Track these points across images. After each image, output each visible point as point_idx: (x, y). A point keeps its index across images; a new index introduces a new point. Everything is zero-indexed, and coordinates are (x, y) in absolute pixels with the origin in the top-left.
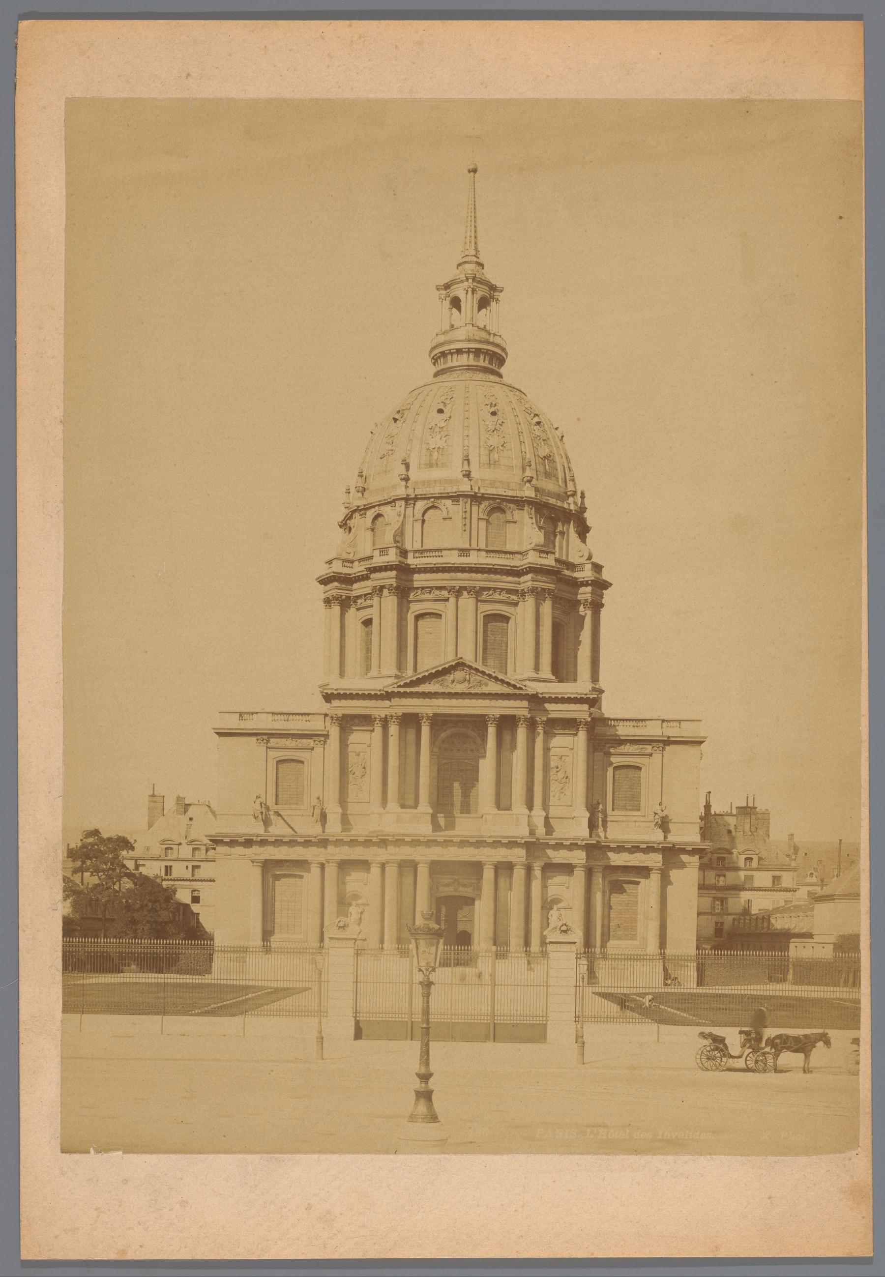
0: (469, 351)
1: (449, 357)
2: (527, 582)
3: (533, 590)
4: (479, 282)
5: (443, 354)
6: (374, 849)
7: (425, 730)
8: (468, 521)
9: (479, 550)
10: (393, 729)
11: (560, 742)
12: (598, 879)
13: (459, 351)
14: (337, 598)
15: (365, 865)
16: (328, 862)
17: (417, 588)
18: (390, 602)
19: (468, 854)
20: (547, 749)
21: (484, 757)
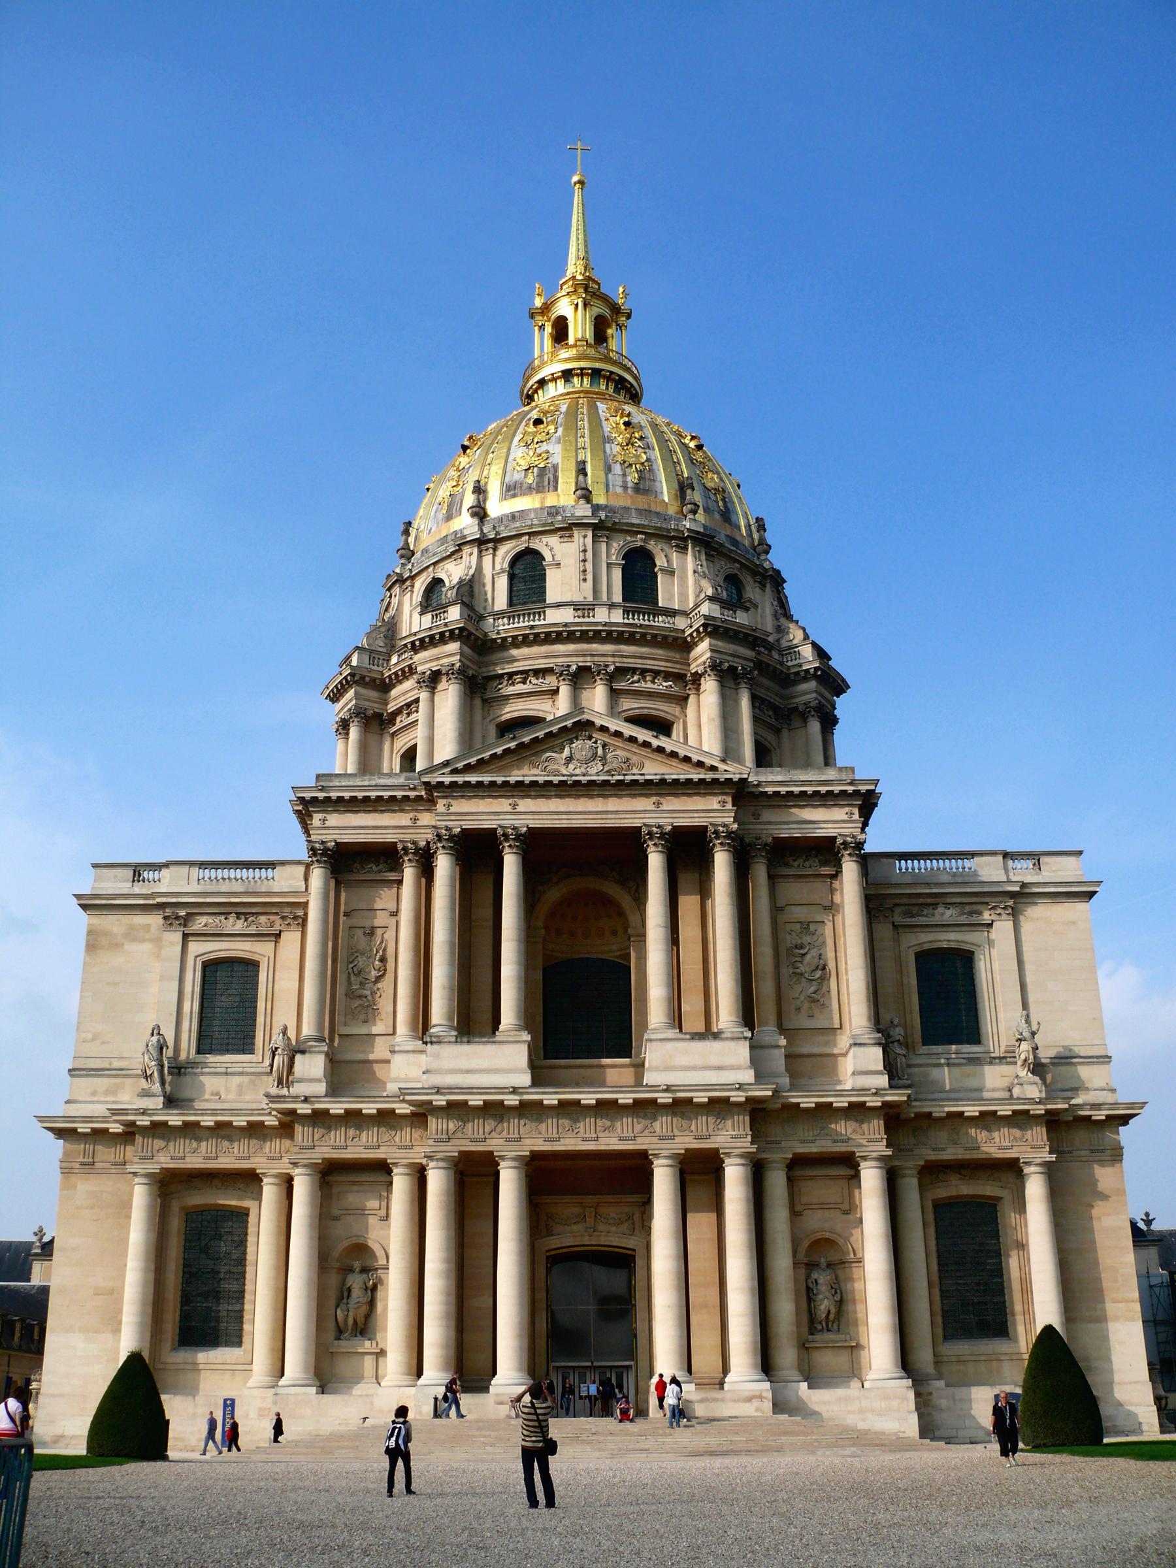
0: (582, 373)
1: (551, 385)
2: (702, 651)
3: (715, 666)
4: (594, 295)
5: (542, 383)
8: (589, 566)
10: (443, 865)
12: (910, 1187)
13: (567, 375)
14: (358, 712)
15: (383, 1168)
17: (502, 676)
18: (449, 696)
19: (612, 1138)
20: (777, 910)
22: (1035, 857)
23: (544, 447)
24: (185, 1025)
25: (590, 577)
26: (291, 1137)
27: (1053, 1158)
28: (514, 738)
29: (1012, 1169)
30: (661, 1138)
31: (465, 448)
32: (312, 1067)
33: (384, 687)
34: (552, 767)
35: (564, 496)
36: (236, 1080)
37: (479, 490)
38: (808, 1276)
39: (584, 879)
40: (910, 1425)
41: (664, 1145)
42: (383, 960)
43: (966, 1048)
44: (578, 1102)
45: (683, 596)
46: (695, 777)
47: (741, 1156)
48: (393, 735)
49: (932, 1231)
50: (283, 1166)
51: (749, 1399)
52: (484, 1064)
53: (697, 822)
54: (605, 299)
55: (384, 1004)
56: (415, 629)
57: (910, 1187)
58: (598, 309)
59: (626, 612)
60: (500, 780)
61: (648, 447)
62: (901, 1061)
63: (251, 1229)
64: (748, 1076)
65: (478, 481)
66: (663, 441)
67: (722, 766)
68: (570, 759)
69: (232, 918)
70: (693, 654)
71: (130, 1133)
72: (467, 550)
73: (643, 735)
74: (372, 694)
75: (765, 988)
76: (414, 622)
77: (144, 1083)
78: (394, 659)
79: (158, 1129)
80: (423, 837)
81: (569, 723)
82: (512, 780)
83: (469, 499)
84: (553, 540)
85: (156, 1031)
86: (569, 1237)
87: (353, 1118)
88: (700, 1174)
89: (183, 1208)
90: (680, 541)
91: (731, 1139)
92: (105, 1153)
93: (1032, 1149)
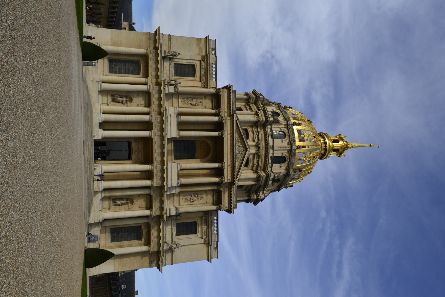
0: (326, 146)
1: (323, 140)
2: (263, 174)
3: (259, 176)
5: (324, 138)
6: (157, 110)
7: (216, 134)
8: (282, 149)
9: (273, 154)
11: (210, 198)
12: (145, 221)
13: (325, 143)
15: (148, 105)
16: (150, 86)
17: (258, 129)
18: (253, 118)
20: (206, 191)
21: (203, 162)
22: (217, 248)
23: (309, 139)
24: (180, 61)
25: (280, 149)
26: (156, 85)
27: (150, 252)
28: (244, 134)
29: (148, 243)
30: (156, 167)
31: (309, 121)
32: (171, 89)
33: (256, 103)
34: (237, 142)
35: (298, 143)
36: (168, 72)
37: (299, 124)
38: (125, 198)
39: (213, 150)
40: (91, 221)
41: (155, 167)
42: (195, 105)
43: (175, 233)
44: (164, 148)
45: (275, 170)
46: (235, 174)
47: (152, 184)
48: (245, 106)
49: (135, 225)
50: (149, 83)
51: (98, 186)
52: (172, 128)
53: (225, 174)
54: (343, 151)
55: (185, 106)
56: (268, 110)
57: (145, 221)
58: (341, 150)
59: (272, 157)
60: (234, 131)
61: (309, 162)
62: (172, 218)
63: (135, 76)
64: (169, 186)
65: (301, 124)
66: (310, 165)
67: (237, 180)
68: (239, 146)
69: (204, 71)
70: (262, 172)
71: (156, 48)
72: (286, 121)
73: (244, 162)
74: (254, 101)
75: (189, 189)
76: (270, 109)
77: (167, 51)
78: (261, 105)
79: (157, 55)
80: (222, 114)
81: (247, 146)
82: (234, 134)
83: (297, 122)
84: (288, 141)
85: (180, 54)
86: (134, 146)
87: (160, 99)
88: (148, 175)
89: (140, 60)
90: (287, 169)
91: (156, 182)
92: (152, 43)
93: (153, 247)
